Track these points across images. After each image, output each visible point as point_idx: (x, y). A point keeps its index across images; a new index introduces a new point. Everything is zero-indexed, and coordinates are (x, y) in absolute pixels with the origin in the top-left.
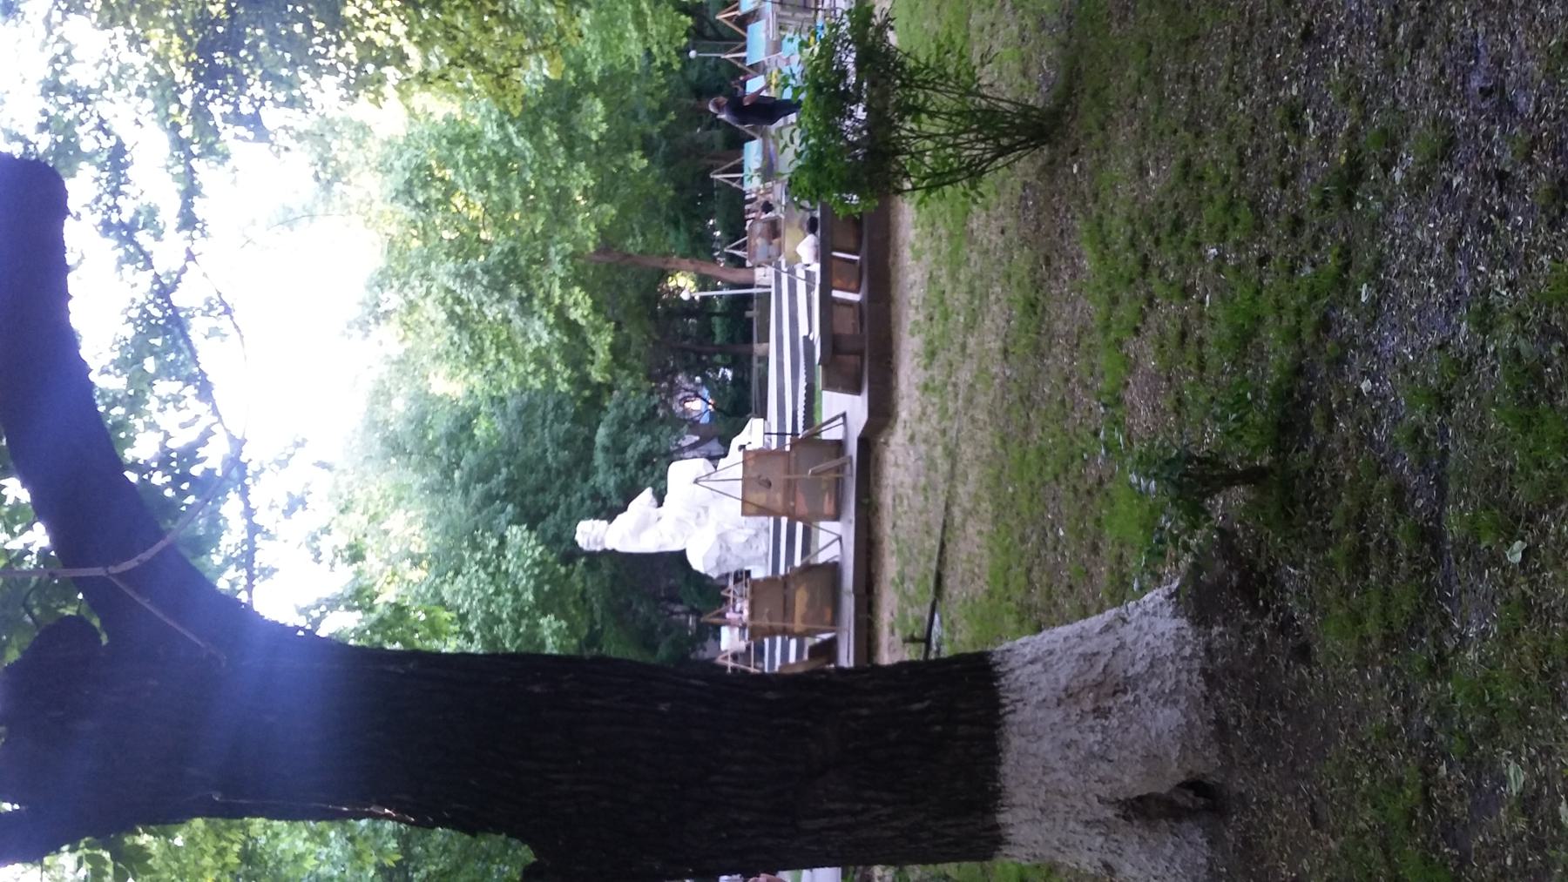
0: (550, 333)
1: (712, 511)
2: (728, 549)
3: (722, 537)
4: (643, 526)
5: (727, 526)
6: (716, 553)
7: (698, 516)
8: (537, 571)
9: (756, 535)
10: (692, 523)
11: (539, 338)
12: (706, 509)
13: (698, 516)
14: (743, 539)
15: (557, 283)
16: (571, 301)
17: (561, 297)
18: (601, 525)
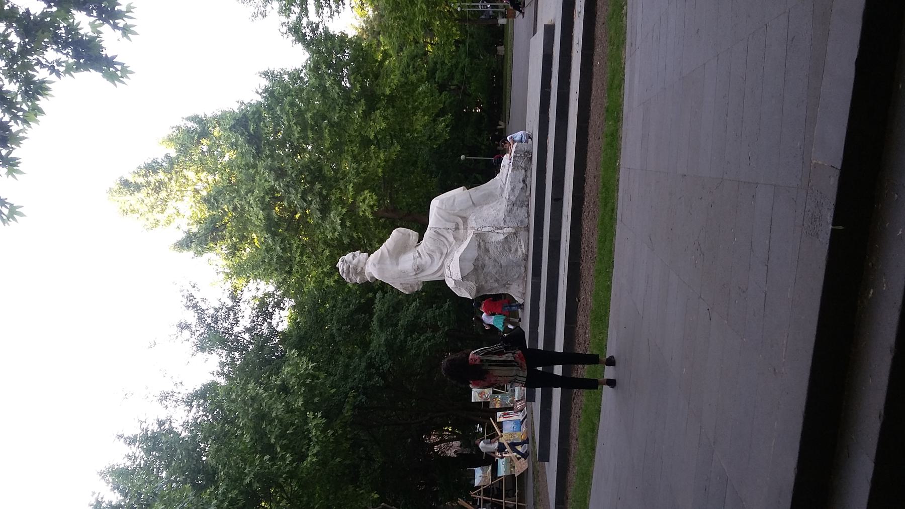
0: (343, 224)
1: (472, 223)
2: (487, 251)
3: (481, 238)
4: (402, 249)
6: (474, 254)
7: (457, 228)
8: (308, 381)
10: (451, 239)
11: (334, 230)
12: (465, 220)
13: (457, 228)
14: (502, 237)
15: (352, 185)
16: (362, 198)
17: (354, 198)
18: (360, 256)
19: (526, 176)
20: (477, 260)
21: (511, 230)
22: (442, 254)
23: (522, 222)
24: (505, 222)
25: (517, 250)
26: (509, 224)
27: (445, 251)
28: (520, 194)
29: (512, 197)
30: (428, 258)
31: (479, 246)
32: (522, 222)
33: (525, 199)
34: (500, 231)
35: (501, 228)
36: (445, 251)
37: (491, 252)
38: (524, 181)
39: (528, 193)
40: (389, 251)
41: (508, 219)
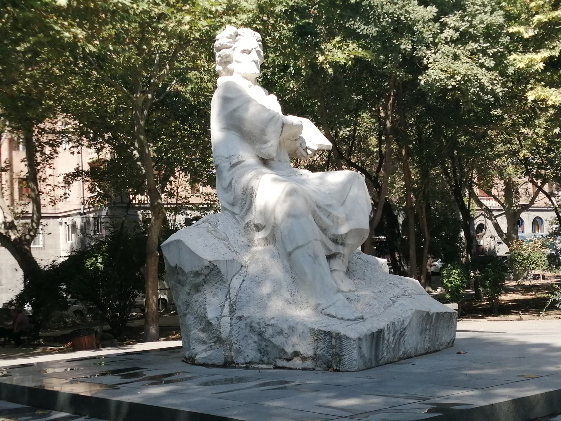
2: (197, 288)
3: (212, 274)
5: (236, 283)
9: (219, 340)
14: (211, 315)
19: (304, 359)
20: (183, 272)
21: (225, 332)
22: (233, 205)
23: (239, 351)
24: (240, 318)
25: (204, 343)
26: (236, 328)
27: (236, 210)
28: (275, 346)
29: (270, 331)
30: (228, 181)
31: (197, 274)
32: (239, 351)
33: (271, 356)
34: (226, 310)
35: (232, 311)
36: (236, 210)
37: (196, 297)
38: (296, 354)
39: (280, 363)
40: (235, 110)
41: (242, 324)
